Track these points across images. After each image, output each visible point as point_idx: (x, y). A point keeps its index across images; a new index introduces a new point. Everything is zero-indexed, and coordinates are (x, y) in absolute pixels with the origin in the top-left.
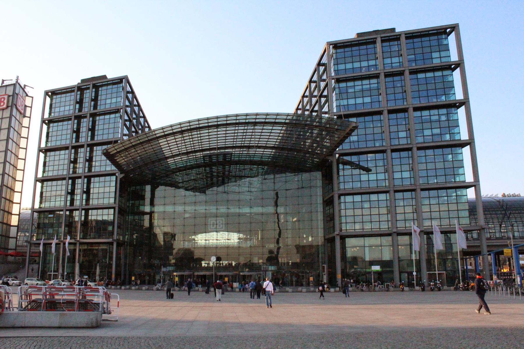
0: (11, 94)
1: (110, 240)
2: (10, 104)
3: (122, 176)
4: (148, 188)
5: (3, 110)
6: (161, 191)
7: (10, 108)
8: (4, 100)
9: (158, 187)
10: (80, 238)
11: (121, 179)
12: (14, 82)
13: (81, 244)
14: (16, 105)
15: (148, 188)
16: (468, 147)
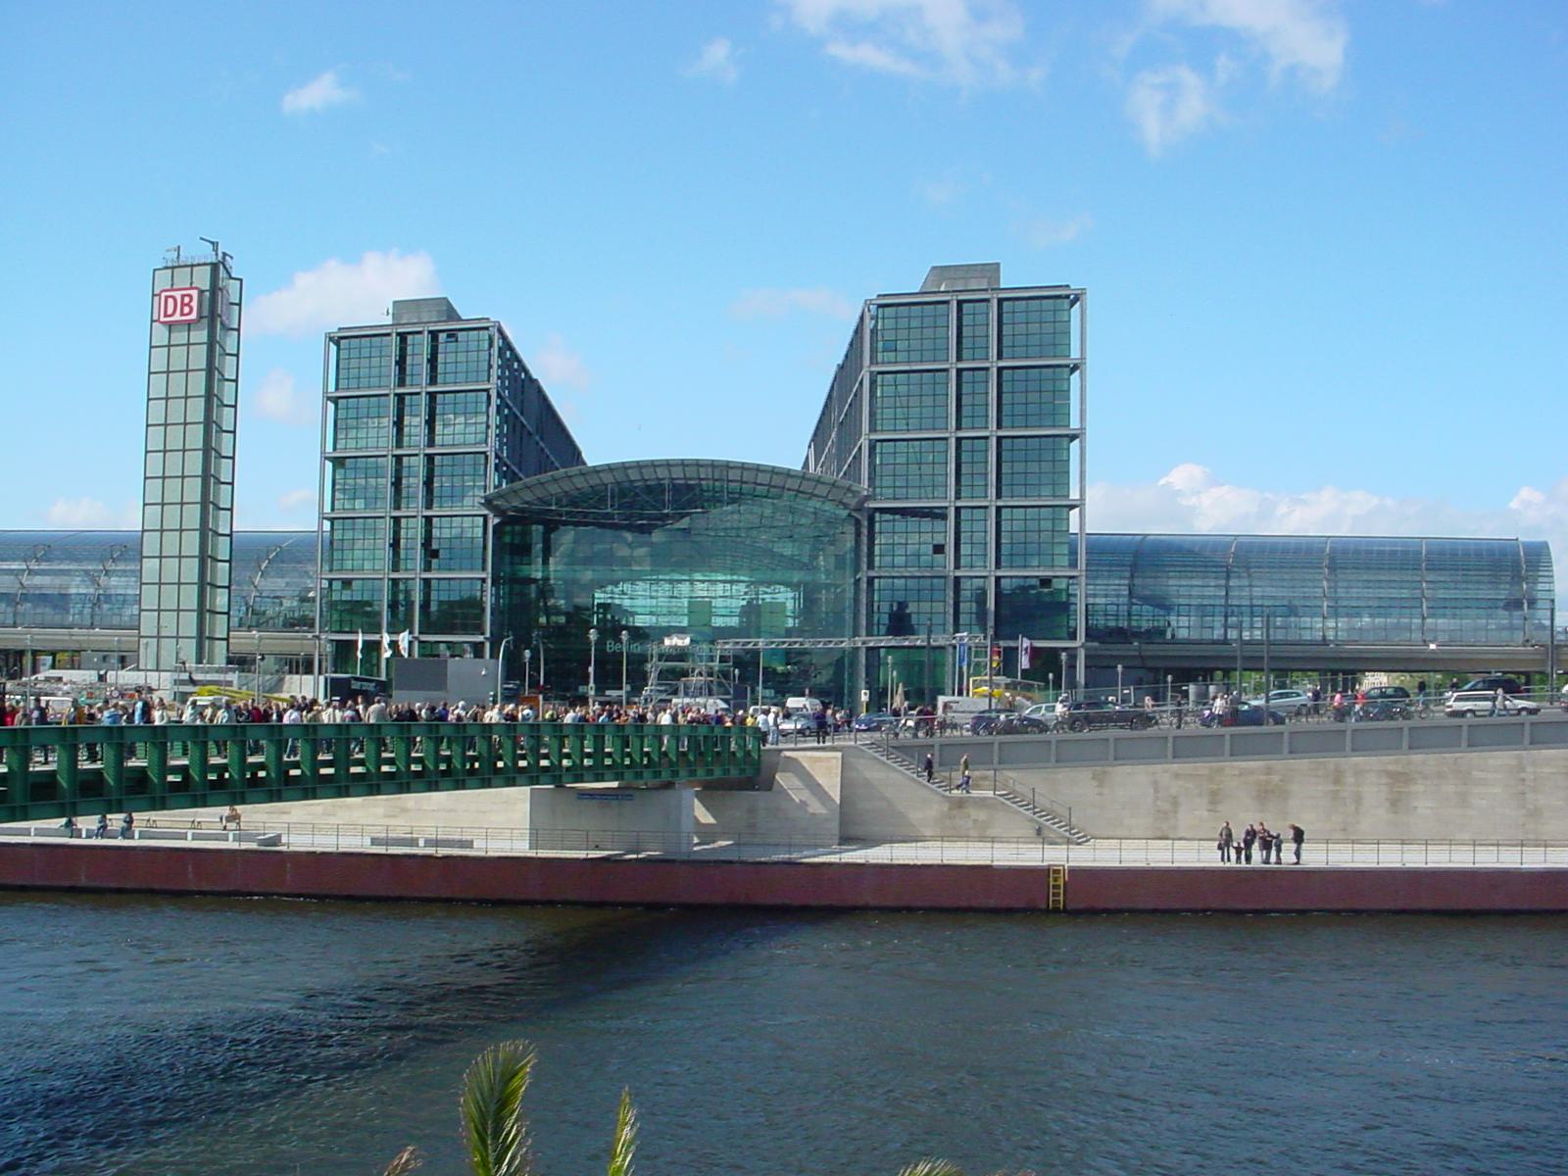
1: (480, 638)
2: (206, 313)
3: (497, 521)
4: (537, 530)
5: (189, 323)
6: (566, 538)
7: (205, 321)
8: (191, 300)
9: (555, 529)
10: (420, 633)
11: (495, 527)
12: (207, 254)
13: (420, 642)
14: (220, 316)
15: (537, 530)
16: (1077, 510)
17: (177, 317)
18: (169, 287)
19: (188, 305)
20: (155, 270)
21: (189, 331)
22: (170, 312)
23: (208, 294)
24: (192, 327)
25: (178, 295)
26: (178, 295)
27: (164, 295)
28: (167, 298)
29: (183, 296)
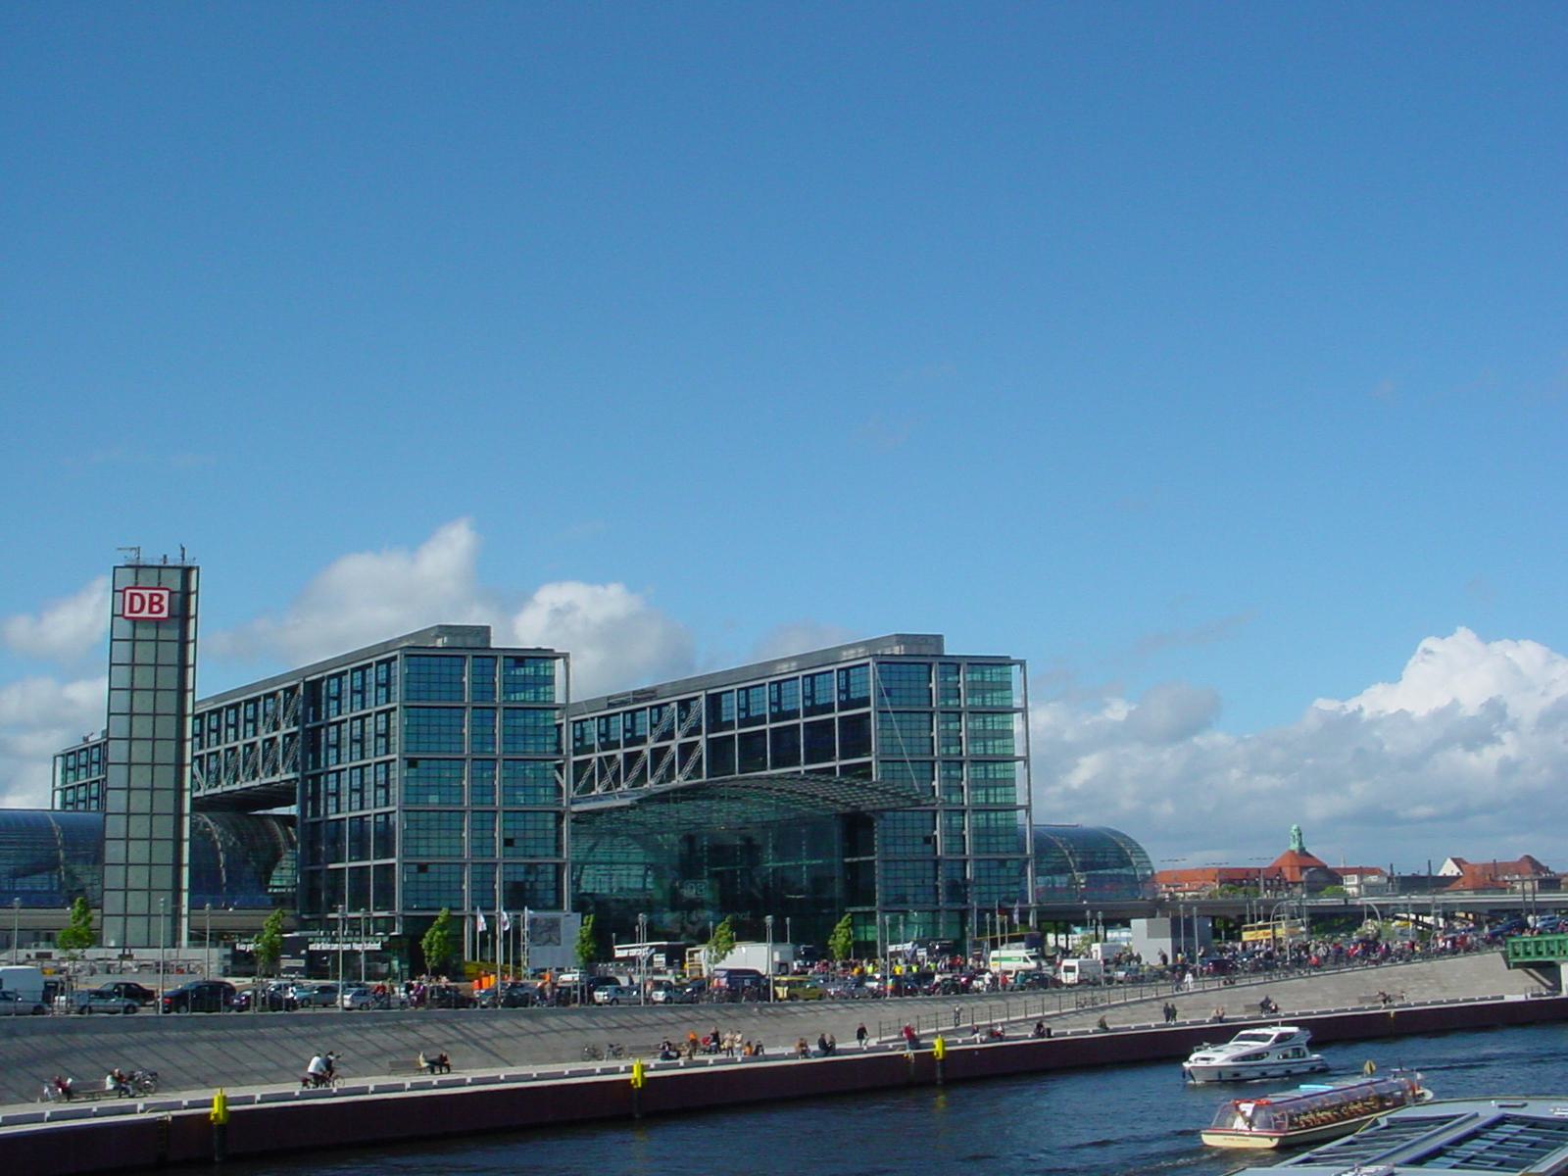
0: (177, 586)
2: (177, 611)
7: (176, 622)
12: (174, 559)
17: (145, 614)
18: (131, 585)
19: (157, 603)
20: (115, 568)
21: (157, 628)
22: (137, 607)
23: (178, 596)
24: (138, 625)
25: (146, 593)
26: (146, 593)
27: (128, 592)
28: (132, 595)
29: (151, 596)
